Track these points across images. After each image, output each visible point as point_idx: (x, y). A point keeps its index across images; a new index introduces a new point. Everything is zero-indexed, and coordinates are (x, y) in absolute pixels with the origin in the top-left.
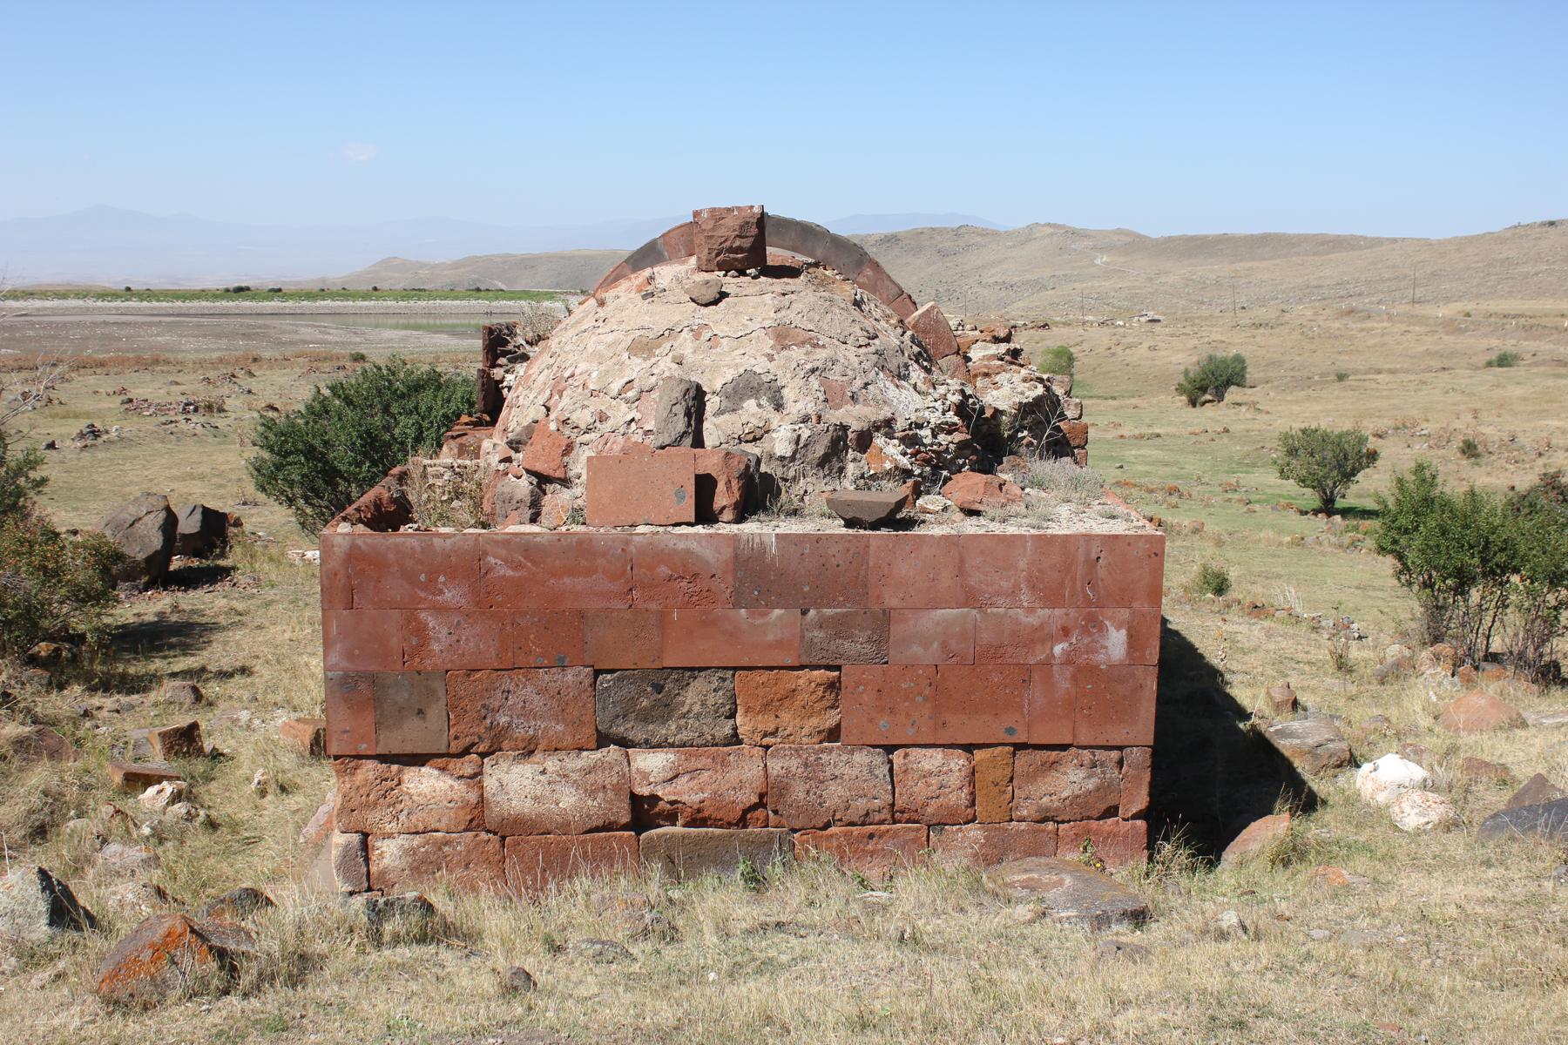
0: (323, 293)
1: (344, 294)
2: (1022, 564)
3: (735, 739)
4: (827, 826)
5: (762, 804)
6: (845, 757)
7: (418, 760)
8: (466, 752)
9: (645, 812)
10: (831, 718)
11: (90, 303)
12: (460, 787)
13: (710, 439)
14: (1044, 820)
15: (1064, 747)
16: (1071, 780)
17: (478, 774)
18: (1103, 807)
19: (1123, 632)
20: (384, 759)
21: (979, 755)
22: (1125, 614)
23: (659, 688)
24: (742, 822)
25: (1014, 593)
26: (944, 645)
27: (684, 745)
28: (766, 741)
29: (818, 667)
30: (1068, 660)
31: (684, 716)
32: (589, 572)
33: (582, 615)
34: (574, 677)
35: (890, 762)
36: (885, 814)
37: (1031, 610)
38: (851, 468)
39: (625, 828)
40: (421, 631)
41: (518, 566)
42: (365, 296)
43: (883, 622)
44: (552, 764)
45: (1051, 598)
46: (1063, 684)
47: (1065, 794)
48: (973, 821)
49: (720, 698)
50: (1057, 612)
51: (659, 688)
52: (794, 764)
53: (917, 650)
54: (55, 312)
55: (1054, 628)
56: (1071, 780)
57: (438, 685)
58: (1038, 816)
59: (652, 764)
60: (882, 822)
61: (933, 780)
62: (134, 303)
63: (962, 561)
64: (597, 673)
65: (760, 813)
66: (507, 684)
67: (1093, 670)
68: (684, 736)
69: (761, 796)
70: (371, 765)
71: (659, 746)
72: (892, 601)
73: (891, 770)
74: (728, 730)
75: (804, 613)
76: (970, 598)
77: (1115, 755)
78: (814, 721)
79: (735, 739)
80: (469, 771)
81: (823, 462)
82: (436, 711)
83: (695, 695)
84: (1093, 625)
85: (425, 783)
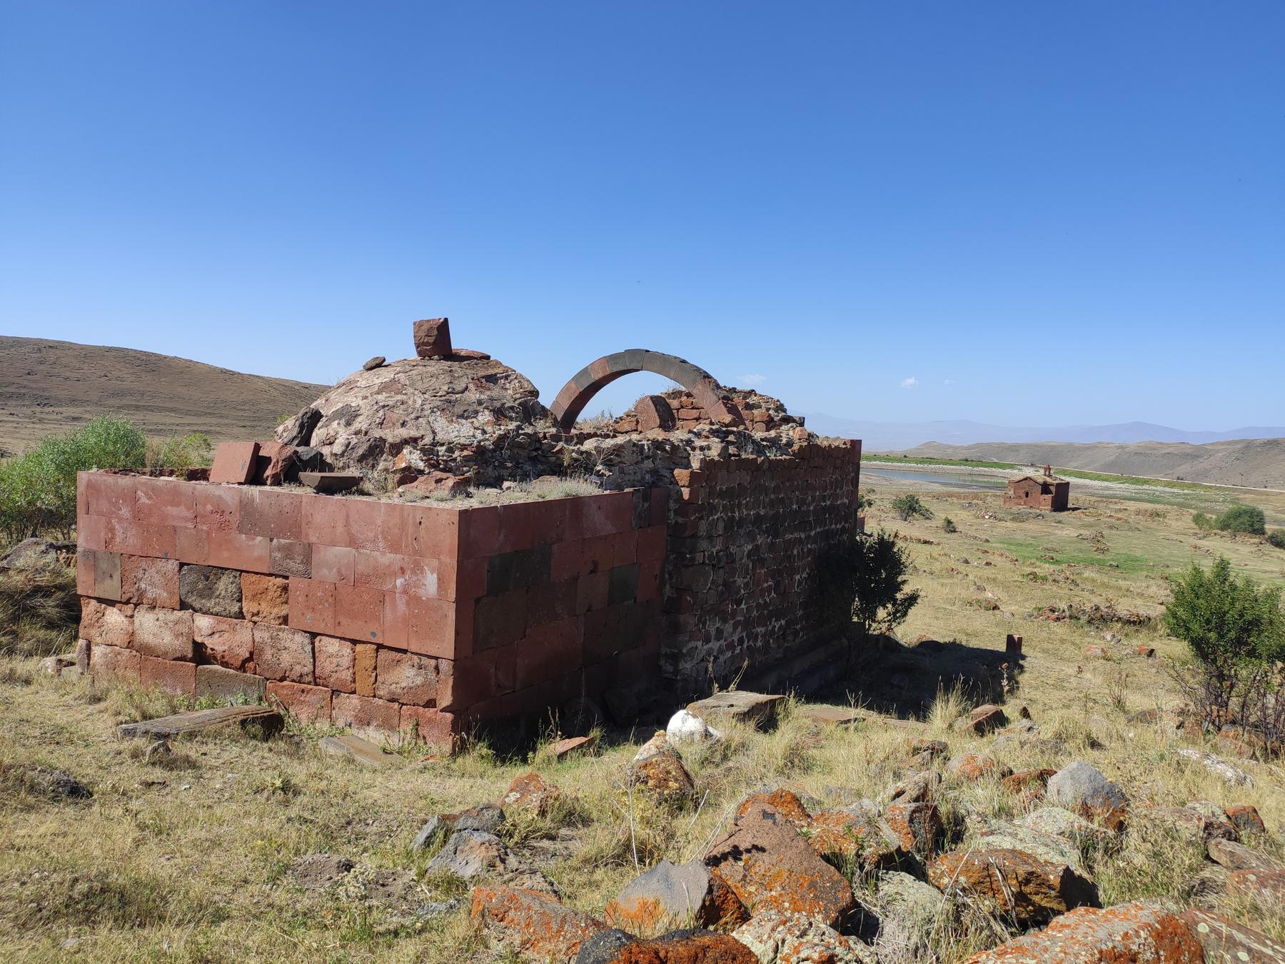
1: (887, 458)
2: (379, 522)
3: (240, 615)
4: (282, 679)
5: (250, 659)
6: (290, 636)
7: (111, 603)
8: (127, 602)
9: (200, 654)
10: (284, 610)
12: (126, 621)
13: (313, 442)
14: (392, 700)
15: (405, 651)
16: (405, 676)
17: (132, 616)
18: (426, 699)
19: (435, 575)
20: (100, 600)
21: (359, 648)
22: (435, 563)
23: (207, 578)
24: (242, 667)
25: (375, 540)
26: (339, 572)
27: (217, 615)
28: (255, 619)
29: (277, 576)
30: (405, 592)
31: (218, 597)
32: (178, 505)
33: (174, 529)
34: (172, 566)
35: (313, 643)
36: (310, 678)
37: (384, 553)
38: (381, 466)
39: (191, 660)
40: (112, 530)
41: (150, 498)
42: (900, 460)
43: (309, 551)
44: (160, 614)
45: (395, 547)
46: (401, 607)
47: (403, 685)
48: (354, 692)
49: (232, 588)
50: (399, 556)
51: (207, 578)
52: (266, 635)
53: (325, 571)
55: (397, 568)
56: (405, 676)
57: (118, 562)
58: (388, 697)
59: (203, 623)
60: (309, 683)
61: (335, 661)
63: (348, 517)
64: (182, 565)
65: (251, 665)
66: (144, 565)
67: (417, 599)
68: (217, 609)
69: (251, 654)
70: (93, 602)
71: (205, 613)
72: (313, 539)
73: (313, 649)
74: (235, 608)
75: (271, 540)
76: (353, 542)
77: (433, 662)
78: (276, 610)
79: (240, 615)
80: (129, 614)
81: (362, 459)
82: (117, 576)
83: (224, 585)
84: (418, 569)
85: (114, 617)
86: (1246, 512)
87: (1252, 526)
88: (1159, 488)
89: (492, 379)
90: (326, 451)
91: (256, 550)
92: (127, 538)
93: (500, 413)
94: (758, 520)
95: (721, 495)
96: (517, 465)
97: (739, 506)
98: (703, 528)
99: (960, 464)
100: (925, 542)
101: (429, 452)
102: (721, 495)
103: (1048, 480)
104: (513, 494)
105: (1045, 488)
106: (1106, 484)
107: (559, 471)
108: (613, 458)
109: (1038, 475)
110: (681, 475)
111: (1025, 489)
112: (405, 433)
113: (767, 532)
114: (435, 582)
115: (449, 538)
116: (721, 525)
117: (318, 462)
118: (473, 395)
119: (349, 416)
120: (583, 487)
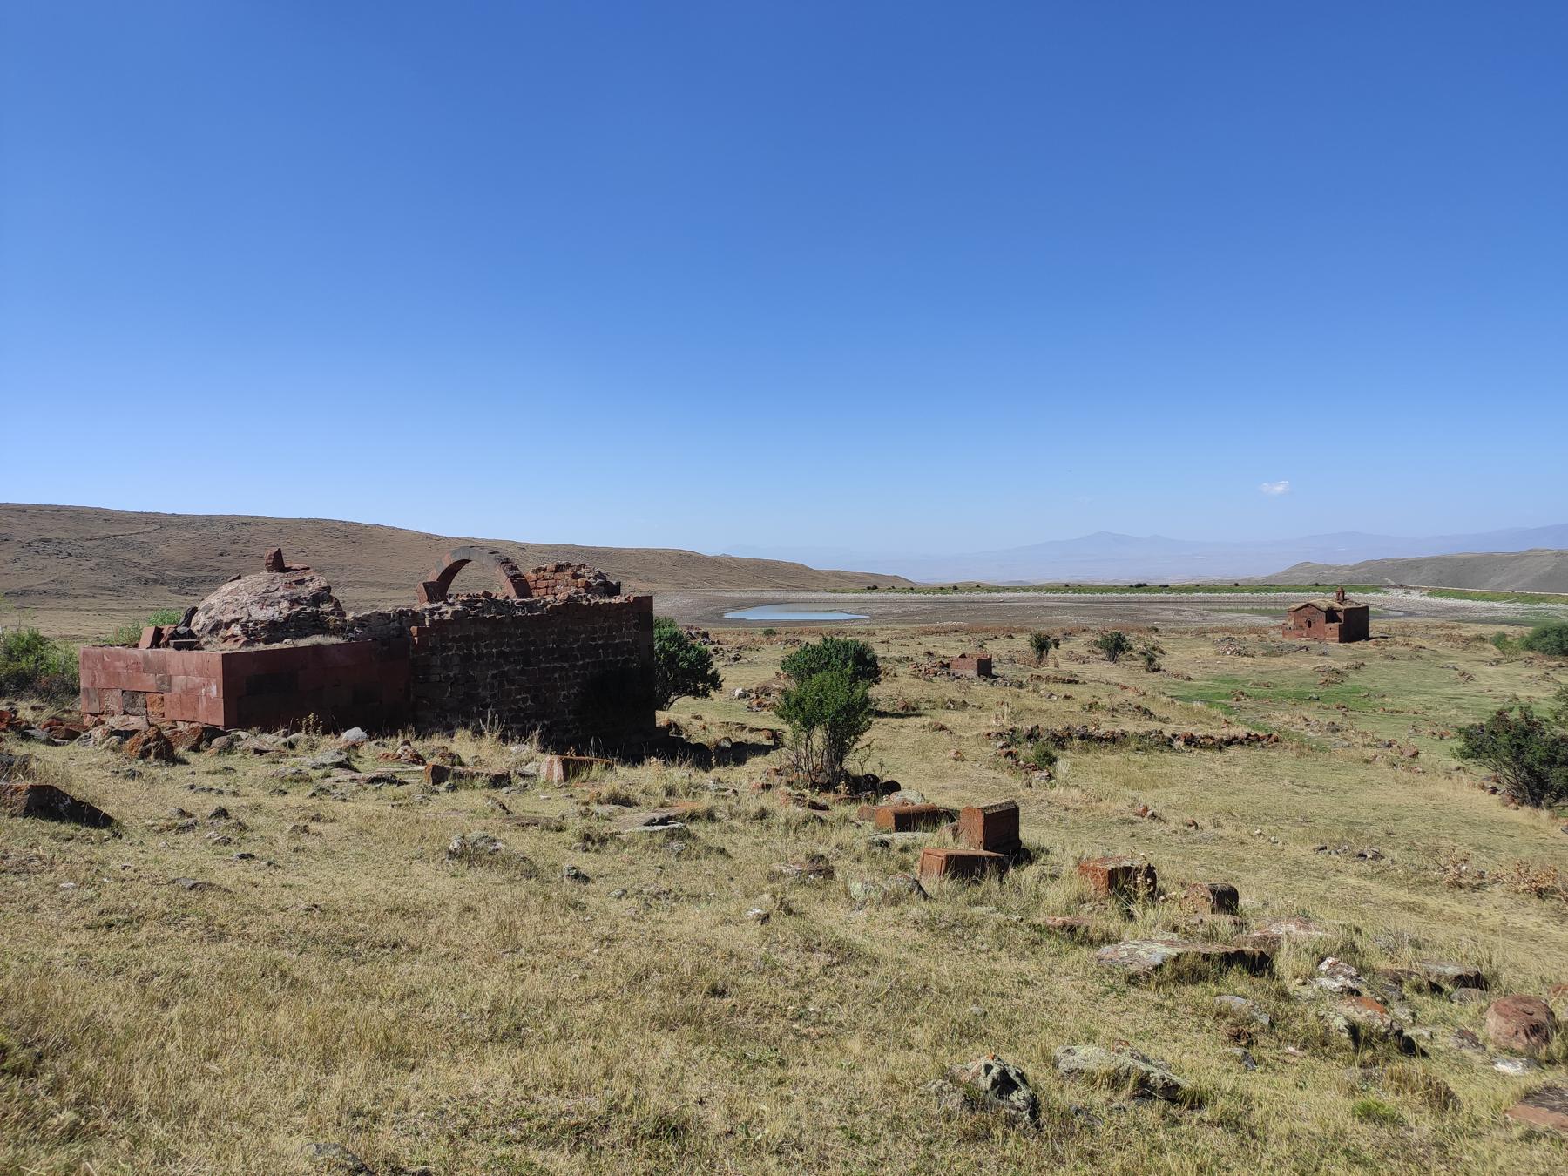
0: (1198, 588)
1: (1213, 588)
11: (1042, 594)
34: (119, 692)
54: (1019, 600)
62: (1069, 595)
76: (186, 674)
81: (210, 632)
83: (140, 700)
86: (1553, 630)
87: (1560, 645)
88: (1561, 606)
89: (301, 582)
90: (194, 629)
91: (150, 681)
92: (101, 681)
93: (294, 602)
94: (501, 654)
95: (454, 640)
96: (301, 630)
97: (477, 647)
98: (436, 660)
99: (1308, 590)
100: (1070, 682)
101: (244, 626)
102: (454, 640)
103: (1336, 605)
104: (287, 644)
105: (1331, 615)
106: (1492, 604)
107: (325, 631)
108: (362, 622)
109: (1326, 600)
110: (414, 629)
111: (1307, 617)
112: (233, 617)
113: (516, 663)
114: (215, 690)
115: (219, 668)
116: (456, 660)
117: (191, 634)
118: (278, 594)
119: (208, 609)
120: (333, 640)
